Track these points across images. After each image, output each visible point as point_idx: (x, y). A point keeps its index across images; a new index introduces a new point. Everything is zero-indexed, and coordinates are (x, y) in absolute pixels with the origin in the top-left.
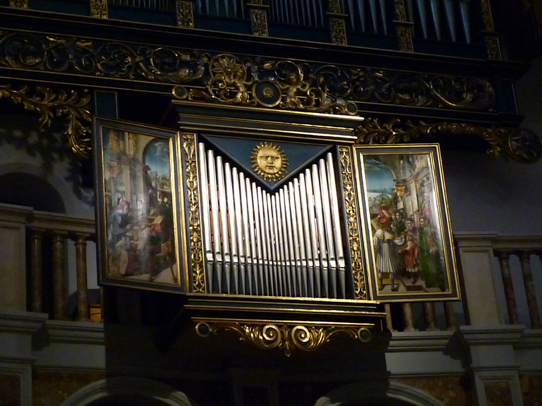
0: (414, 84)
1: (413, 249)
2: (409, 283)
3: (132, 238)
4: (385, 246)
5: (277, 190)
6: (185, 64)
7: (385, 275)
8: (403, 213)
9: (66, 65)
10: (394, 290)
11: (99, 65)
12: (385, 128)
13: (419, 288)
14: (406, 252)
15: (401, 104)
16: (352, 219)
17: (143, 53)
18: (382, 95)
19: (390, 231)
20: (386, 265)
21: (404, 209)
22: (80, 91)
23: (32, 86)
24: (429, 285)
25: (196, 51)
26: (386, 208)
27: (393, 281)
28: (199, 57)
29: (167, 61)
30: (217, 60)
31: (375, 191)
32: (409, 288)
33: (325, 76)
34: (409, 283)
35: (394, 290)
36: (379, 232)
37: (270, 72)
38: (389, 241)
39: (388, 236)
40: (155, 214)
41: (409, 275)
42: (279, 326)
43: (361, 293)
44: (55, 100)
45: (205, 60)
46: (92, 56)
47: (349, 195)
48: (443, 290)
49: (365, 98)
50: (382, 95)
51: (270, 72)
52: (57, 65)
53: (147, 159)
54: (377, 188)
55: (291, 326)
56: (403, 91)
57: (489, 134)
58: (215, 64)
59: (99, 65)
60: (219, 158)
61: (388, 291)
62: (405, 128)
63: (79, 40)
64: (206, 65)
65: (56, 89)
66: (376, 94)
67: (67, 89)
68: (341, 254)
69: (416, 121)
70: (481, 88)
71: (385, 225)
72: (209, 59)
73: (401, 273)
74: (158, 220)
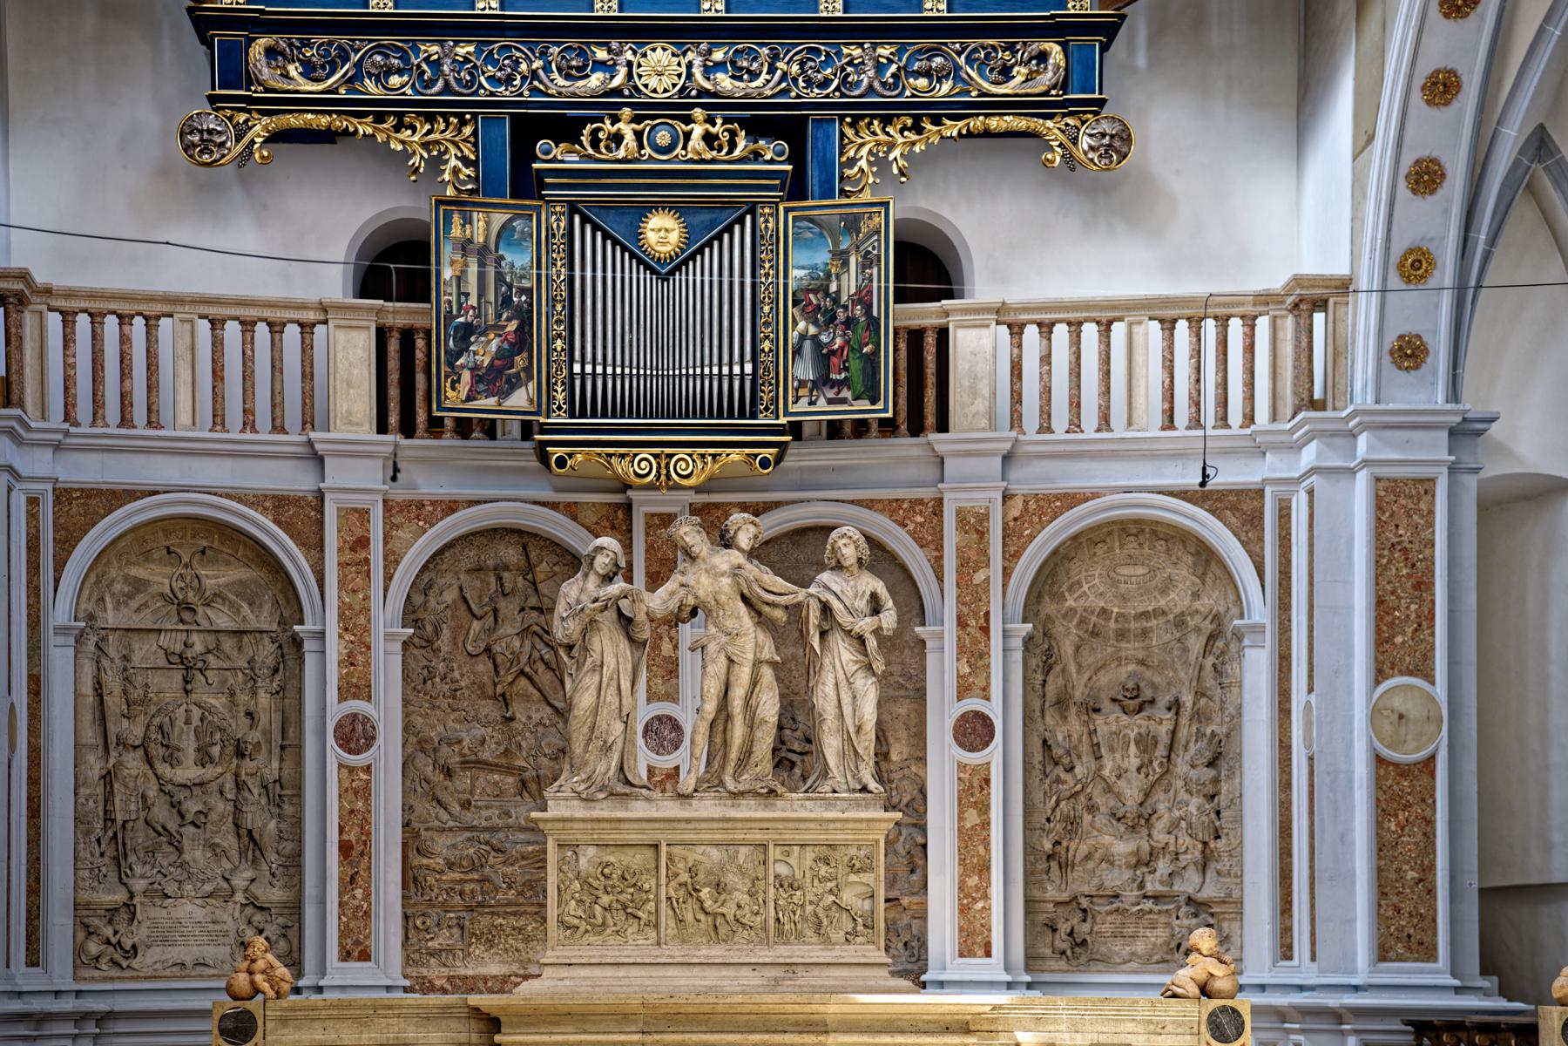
0: (938, 61)
1: (842, 349)
2: (831, 394)
3: (475, 353)
4: (807, 344)
5: (672, 273)
6: (600, 65)
7: (802, 384)
8: (836, 300)
9: (440, 84)
10: (811, 403)
11: (482, 79)
12: (888, 134)
13: (844, 401)
14: (833, 353)
15: (913, 96)
16: (766, 309)
17: (543, 54)
18: (884, 84)
19: (815, 323)
20: (804, 370)
21: (838, 292)
22: (460, 116)
23: (400, 115)
24: (856, 399)
25: (614, 44)
26: (815, 292)
27: (811, 391)
28: (620, 53)
29: (574, 63)
30: (644, 55)
31: (803, 268)
32: (830, 402)
33: (802, 64)
34: (831, 394)
35: (811, 403)
36: (802, 325)
37: (720, 66)
38: (815, 338)
39: (812, 330)
40: (509, 319)
41: (834, 384)
42: (656, 456)
43: (767, 409)
44: (429, 132)
45: (629, 55)
46: (475, 66)
47: (767, 275)
48: (873, 403)
49: (857, 93)
50: (884, 84)
51: (720, 66)
52: (429, 84)
53: (501, 245)
54: (806, 263)
55: (670, 456)
56: (918, 74)
57: (1052, 128)
58: (642, 61)
59: (482, 79)
60: (599, 234)
61: (803, 405)
62: (918, 129)
63: (456, 43)
64: (629, 64)
65: (430, 118)
66: (876, 84)
67: (443, 115)
68: (748, 356)
69: (936, 121)
70: (1043, 57)
71: (811, 314)
72: (635, 53)
73: (823, 381)
74: (512, 326)
